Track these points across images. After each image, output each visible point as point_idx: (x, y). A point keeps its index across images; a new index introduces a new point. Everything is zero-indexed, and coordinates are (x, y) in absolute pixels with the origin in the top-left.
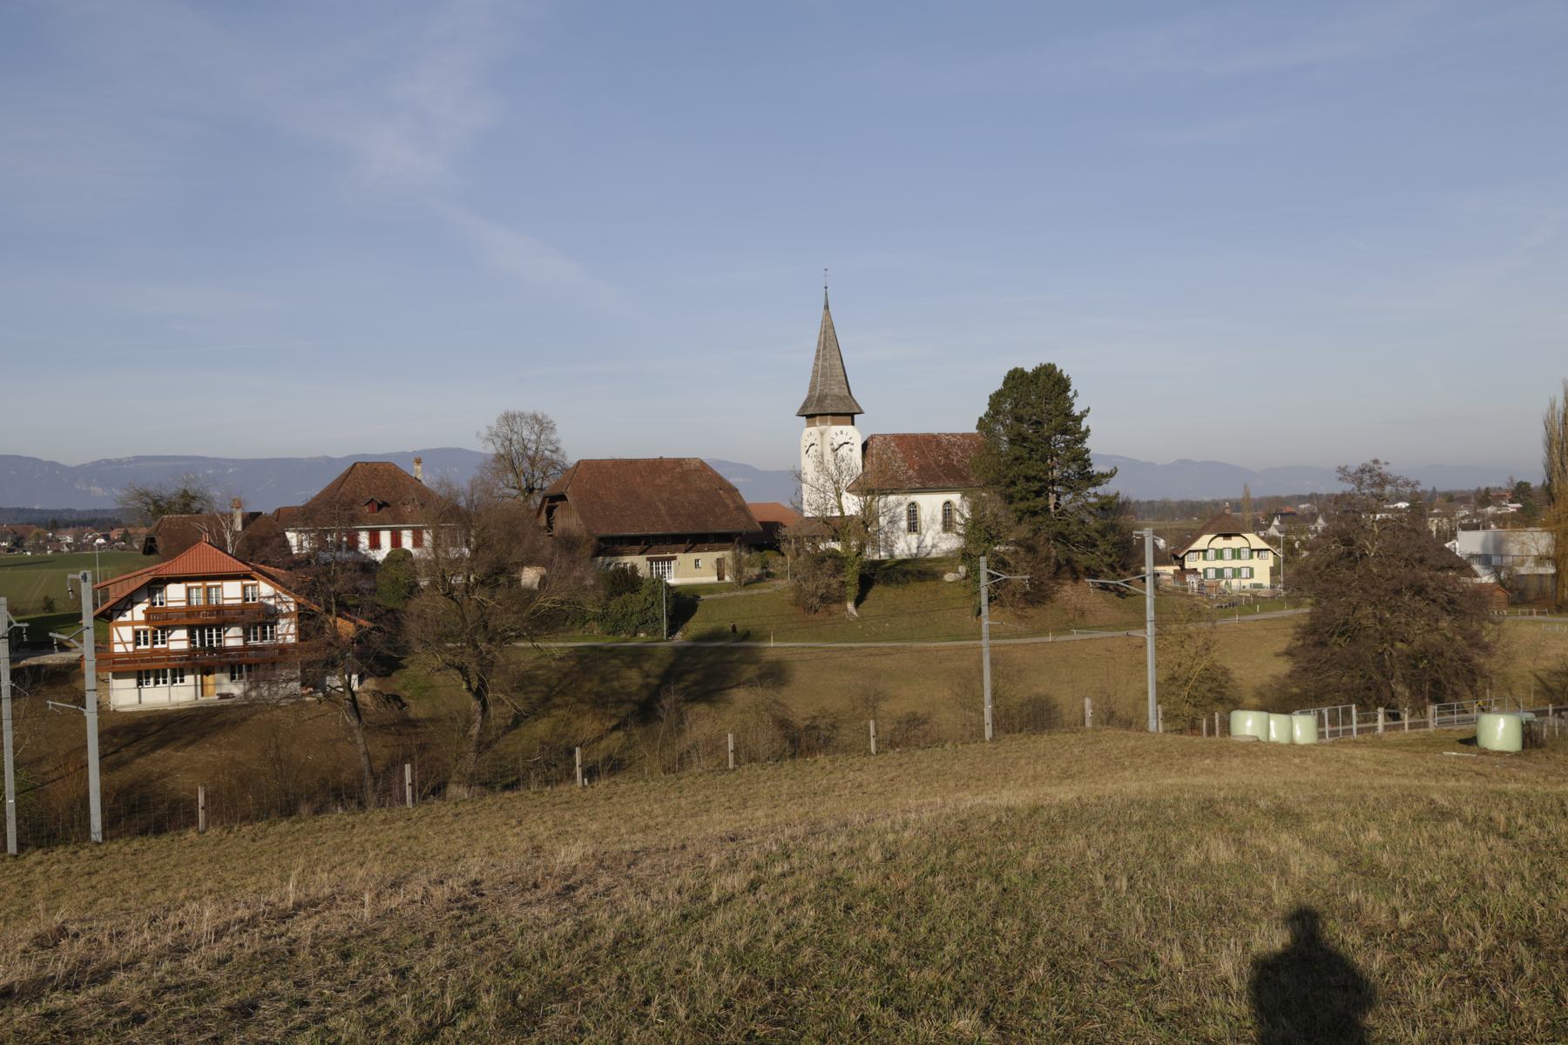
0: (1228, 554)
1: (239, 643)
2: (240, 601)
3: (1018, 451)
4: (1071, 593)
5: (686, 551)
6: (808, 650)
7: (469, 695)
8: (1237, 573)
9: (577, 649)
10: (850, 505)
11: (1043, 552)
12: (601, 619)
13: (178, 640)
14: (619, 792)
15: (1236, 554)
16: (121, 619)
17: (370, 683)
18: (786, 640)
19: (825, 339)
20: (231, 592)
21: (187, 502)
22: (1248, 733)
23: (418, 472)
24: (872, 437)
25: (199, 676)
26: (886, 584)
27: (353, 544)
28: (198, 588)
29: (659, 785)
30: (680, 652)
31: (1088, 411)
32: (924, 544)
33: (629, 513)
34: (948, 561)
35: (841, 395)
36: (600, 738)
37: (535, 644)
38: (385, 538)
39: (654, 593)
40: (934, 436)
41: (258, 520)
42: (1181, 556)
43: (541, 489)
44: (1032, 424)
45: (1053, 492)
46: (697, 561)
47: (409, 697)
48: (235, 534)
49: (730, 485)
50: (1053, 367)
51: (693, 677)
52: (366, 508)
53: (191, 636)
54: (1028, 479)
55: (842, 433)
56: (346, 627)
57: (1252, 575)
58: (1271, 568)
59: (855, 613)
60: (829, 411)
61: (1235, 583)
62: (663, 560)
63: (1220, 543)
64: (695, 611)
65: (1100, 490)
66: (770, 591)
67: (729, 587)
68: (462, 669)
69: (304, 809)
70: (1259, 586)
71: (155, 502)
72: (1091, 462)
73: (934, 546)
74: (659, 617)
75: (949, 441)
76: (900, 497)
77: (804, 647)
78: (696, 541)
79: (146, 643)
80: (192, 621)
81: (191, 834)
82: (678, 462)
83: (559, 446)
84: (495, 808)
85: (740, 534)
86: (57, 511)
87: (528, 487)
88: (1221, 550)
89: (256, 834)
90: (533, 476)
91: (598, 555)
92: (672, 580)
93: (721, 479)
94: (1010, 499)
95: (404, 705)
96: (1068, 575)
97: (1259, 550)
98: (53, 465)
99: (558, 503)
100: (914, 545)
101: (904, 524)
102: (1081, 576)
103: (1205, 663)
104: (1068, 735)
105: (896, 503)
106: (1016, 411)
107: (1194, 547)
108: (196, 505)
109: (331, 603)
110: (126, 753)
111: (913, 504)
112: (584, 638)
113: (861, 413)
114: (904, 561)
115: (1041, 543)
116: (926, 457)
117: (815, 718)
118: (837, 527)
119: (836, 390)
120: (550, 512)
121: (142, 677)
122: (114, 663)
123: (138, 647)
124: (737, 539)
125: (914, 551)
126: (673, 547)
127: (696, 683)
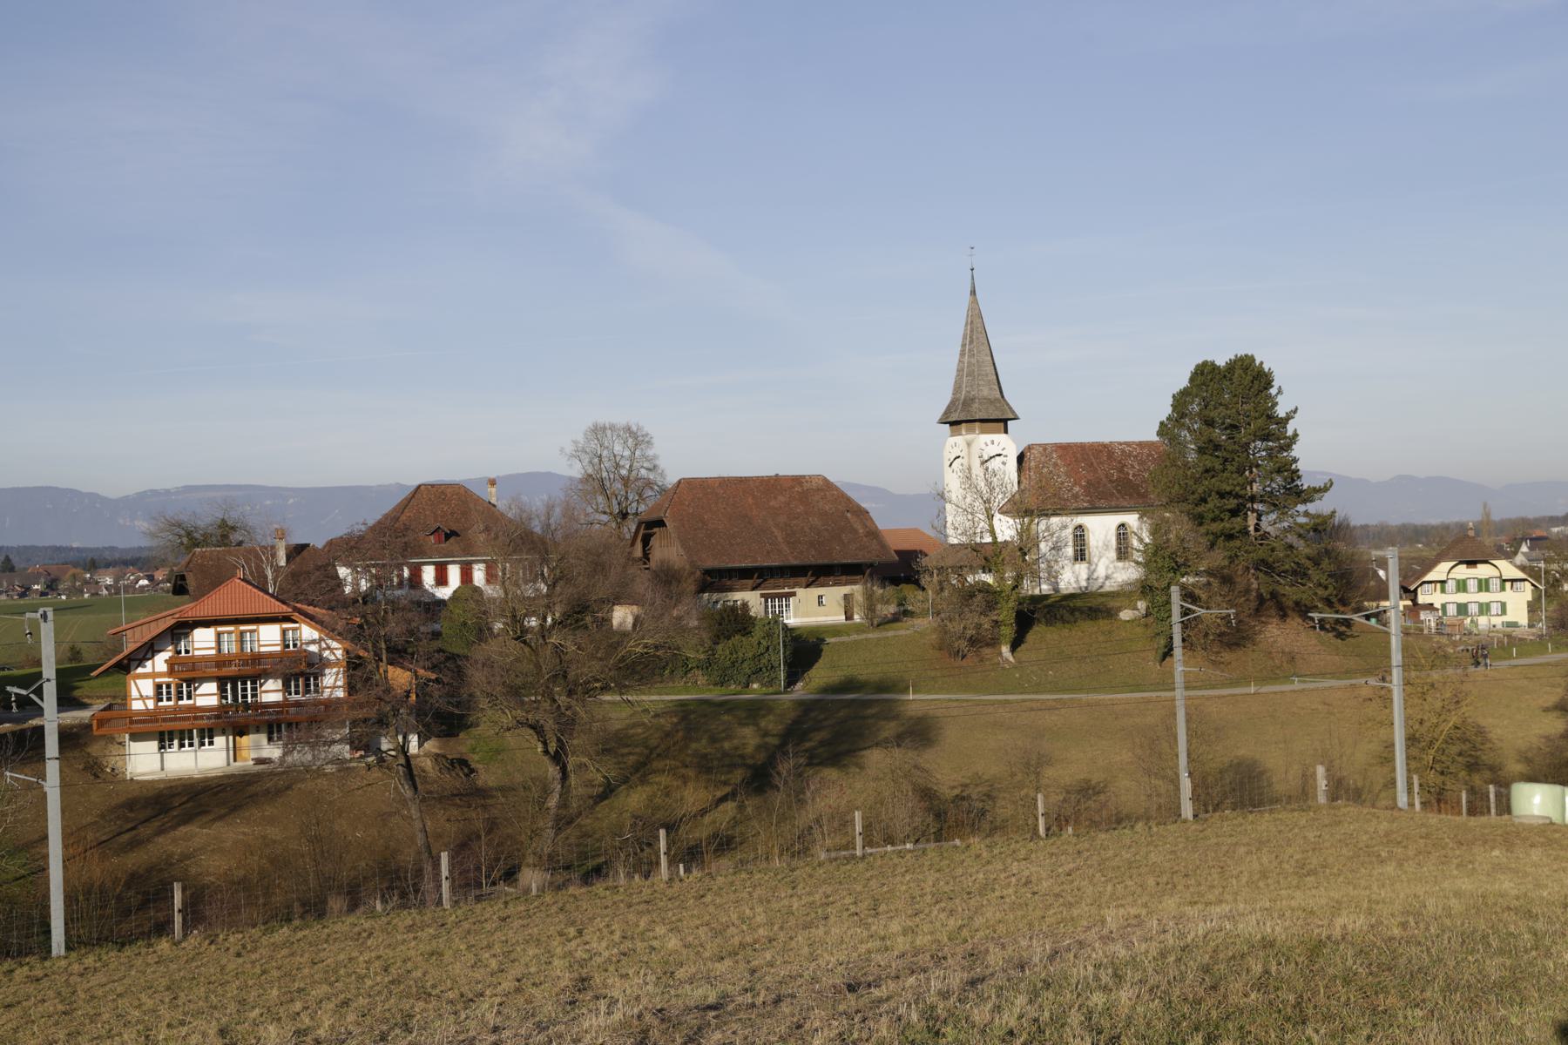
0: (1472, 585)
1: (213, 701)
2: (278, 648)
3: (1209, 462)
4: (1278, 634)
5: (808, 586)
6: (955, 704)
7: (546, 759)
8: (1484, 609)
9: (682, 704)
10: (1003, 529)
11: (1241, 582)
12: (707, 666)
13: (207, 695)
14: (715, 888)
15: (1484, 585)
16: (140, 670)
17: (431, 745)
18: (929, 692)
19: (972, 331)
20: (269, 637)
21: (225, 532)
22: (1536, 812)
23: (491, 494)
24: (1029, 448)
25: (231, 738)
26: (1049, 623)
27: (416, 580)
28: (229, 633)
29: (766, 878)
31: (1295, 411)
32: (1095, 576)
33: (739, 540)
34: (1124, 595)
35: (992, 397)
36: (703, 812)
37: (625, 697)
38: (454, 573)
39: (769, 635)
40: (1105, 446)
41: (305, 553)
42: (1412, 588)
43: (636, 514)
44: (1226, 429)
45: (1253, 511)
46: (820, 597)
47: (478, 762)
48: (277, 569)
49: (859, 507)
50: (1252, 359)
51: (818, 736)
52: (432, 537)
53: (222, 691)
54: (1222, 495)
55: (993, 442)
56: (400, 677)
57: (1504, 611)
58: (1528, 602)
59: (1011, 659)
60: (977, 418)
61: (1483, 621)
62: (780, 596)
63: (1462, 572)
64: (820, 657)
65: (1312, 508)
66: (908, 632)
67: (859, 629)
68: (537, 729)
69: (336, 903)
70: (1514, 625)
71: (189, 534)
72: (1300, 473)
73: (1107, 578)
74: (776, 664)
75: (1123, 451)
76: (1064, 518)
77: (950, 700)
78: (819, 573)
79: (169, 699)
80: (226, 671)
81: (164, 945)
82: (798, 480)
83: (657, 462)
84: (554, 909)
85: (871, 565)
86: (98, 549)
87: (621, 511)
88: (1464, 581)
89: (244, 947)
90: (627, 498)
91: (702, 590)
92: (791, 620)
93: (849, 500)
94: (1199, 519)
95: (472, 771)
96: (1273, 612)
97: (1513, 581)
98: (93, 497)
99: (656, 530)
100: (1084, 576)
101: (1070, 551)
102: (1290, 612)
103: (1454, 719)
104: (1296, 814)
105: (1060, 526)
106: (1206, 412)
107: (1428, 578)
108: (236, 537)
110: (144, 831)
111: (1080, 526)
114: (1072, 596)
115: (1240, 572)
116: (1095, 471)
117: (966, 786)
118: (989, 555)
119: (985, 392)
120: (646, 541)
121: (164, 739)
122: (132, 722)
123: (160, 704)
124: (868, 571)
125: (1084, 584)
126: (792, 580)
127: (822, 743)
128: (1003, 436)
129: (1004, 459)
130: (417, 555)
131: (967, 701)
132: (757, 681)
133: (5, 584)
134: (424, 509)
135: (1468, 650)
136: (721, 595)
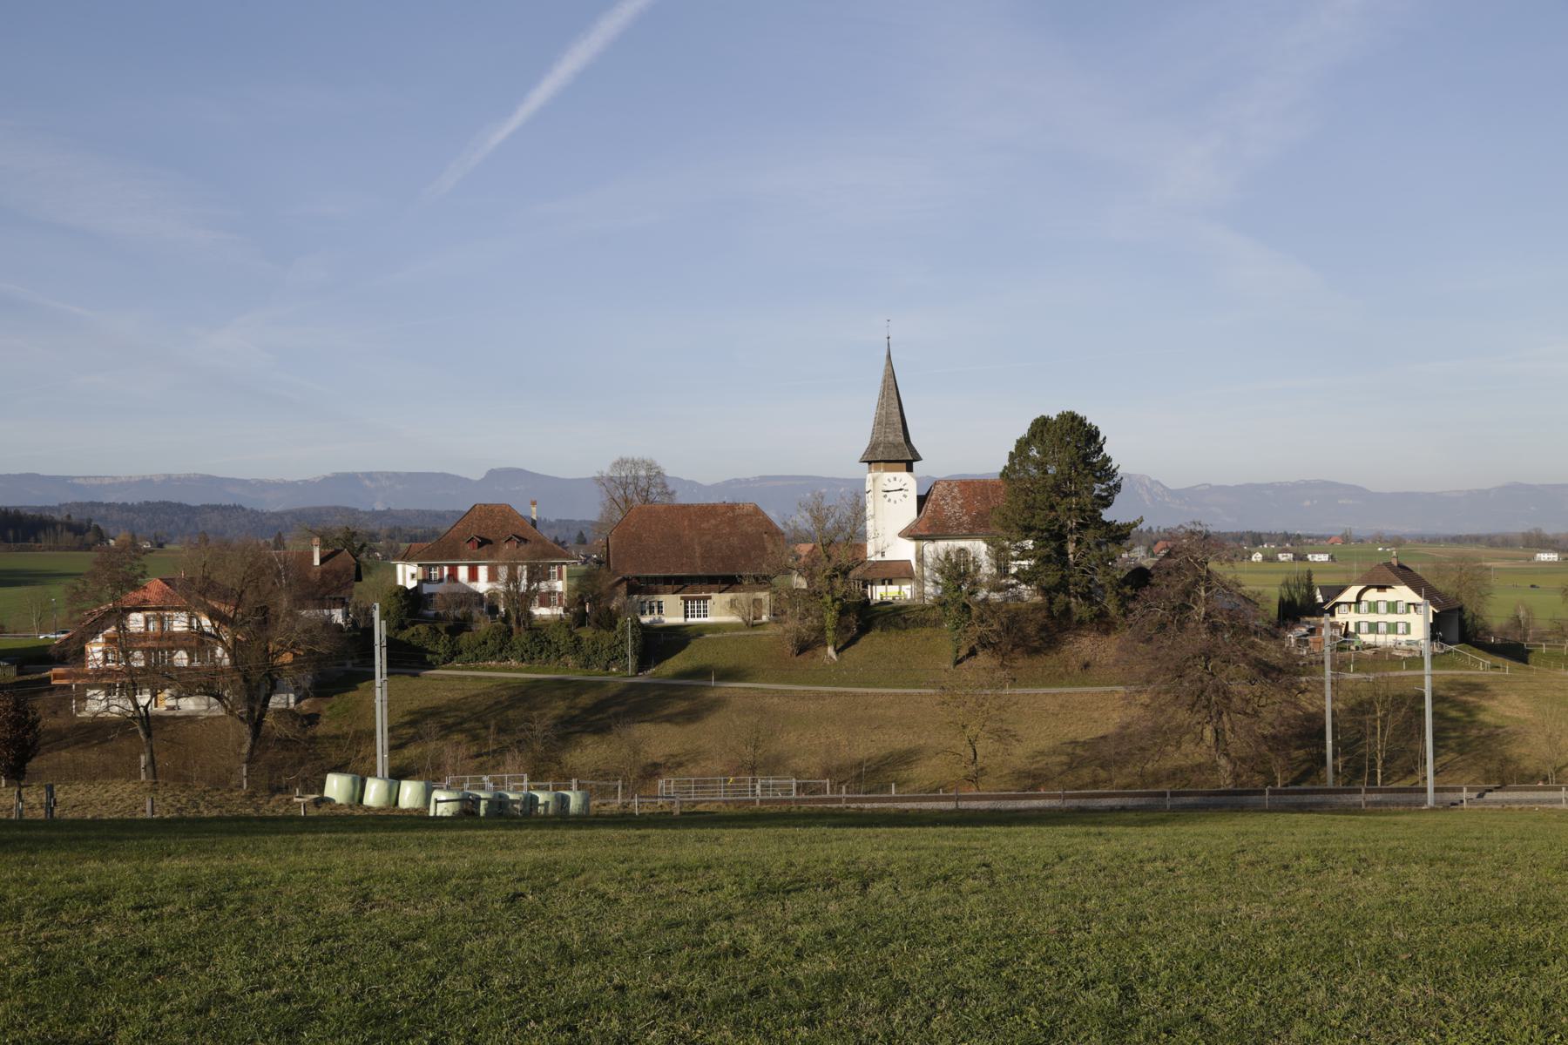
0: (1382, 607)
4: (1085, 645)
5: (720, 592)
6: (742, 691)
8: (1392, 628)
18: (777, 681)
20: (179, 624)
27: (453, 576)
30: (633, 686)
33: (662, 554)
38: (483, 572)
55: (895, 479)
57: (1408, 631)
59: (834, 657)
61: (1391, 638)
62: (699, 599)
63: (1372, 595)
78: (728, 582)
82: (732, 507)
93: (769, 523)
107: (1340, 599)
109: (145, 641)
112: (556, 671)
113: (920, 459)
119: (891, 439)
126: (706, 587)
128: (905, 475)
129: (906, 493)
130: (452, 558)
131: (758, 689)
132: (615, 665)
134: (472, 523)
136: (648, 597)
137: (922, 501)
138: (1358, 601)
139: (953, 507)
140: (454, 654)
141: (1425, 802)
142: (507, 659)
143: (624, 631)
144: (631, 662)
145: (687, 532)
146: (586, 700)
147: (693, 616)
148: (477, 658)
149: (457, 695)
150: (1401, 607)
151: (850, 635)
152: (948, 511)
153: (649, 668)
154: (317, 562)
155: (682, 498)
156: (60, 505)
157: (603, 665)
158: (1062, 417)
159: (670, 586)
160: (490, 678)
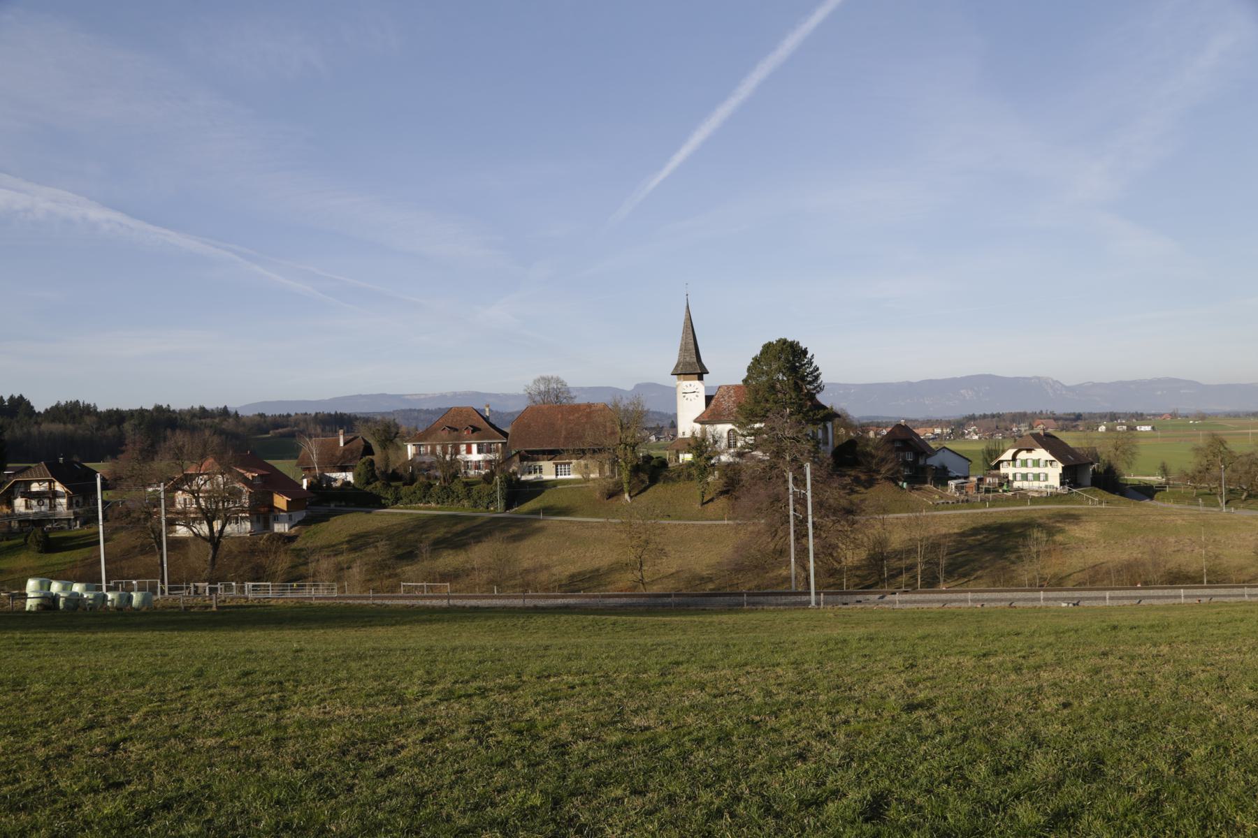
0: (1030, 463)
59: (629, 500)
61: (1036, 484)
62: (565, 464)
63: (1023, 455)
82: (589, 406)
107: (1001, 458)
113: (708, 373)
119: (688, 359)
128: (698, 382)
133: (666, 434)
135: (948, 503)
137: (709, 399)
138: (1014, 458)
139: (728, 402)
140: (397, 500)
141: (810, 603)
142: (429, 502)
143: (496, 484)
144: (500, 504)
145: (559, 422)
146: (459, 528)
147: (561, 475)
148: (411, 502)
149: (384, 525)
150: (1042, 463)
151: (643, 486)
152: (725, 405)
153: (512, 508)
154: (342, 444)
155: (581, 400)
156: (394, 411)
157: (485, 505)
158: (778, 341)
159: (545, 456)
160: (411, 514)
